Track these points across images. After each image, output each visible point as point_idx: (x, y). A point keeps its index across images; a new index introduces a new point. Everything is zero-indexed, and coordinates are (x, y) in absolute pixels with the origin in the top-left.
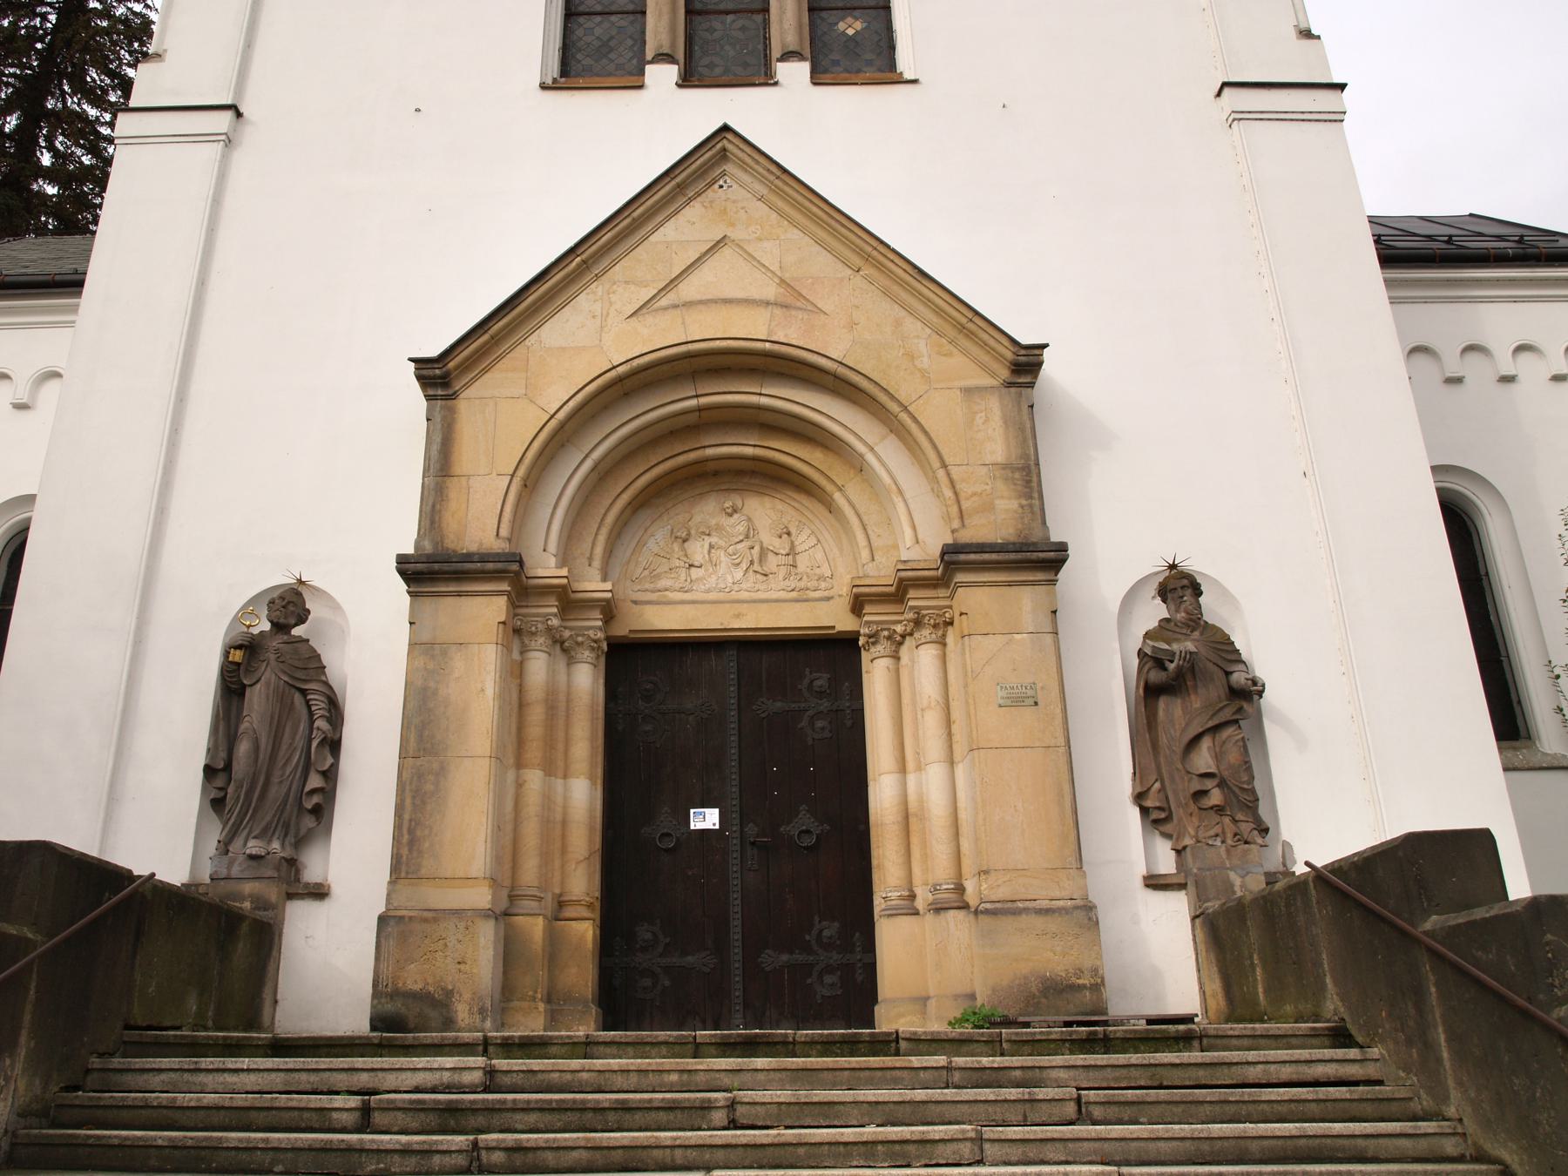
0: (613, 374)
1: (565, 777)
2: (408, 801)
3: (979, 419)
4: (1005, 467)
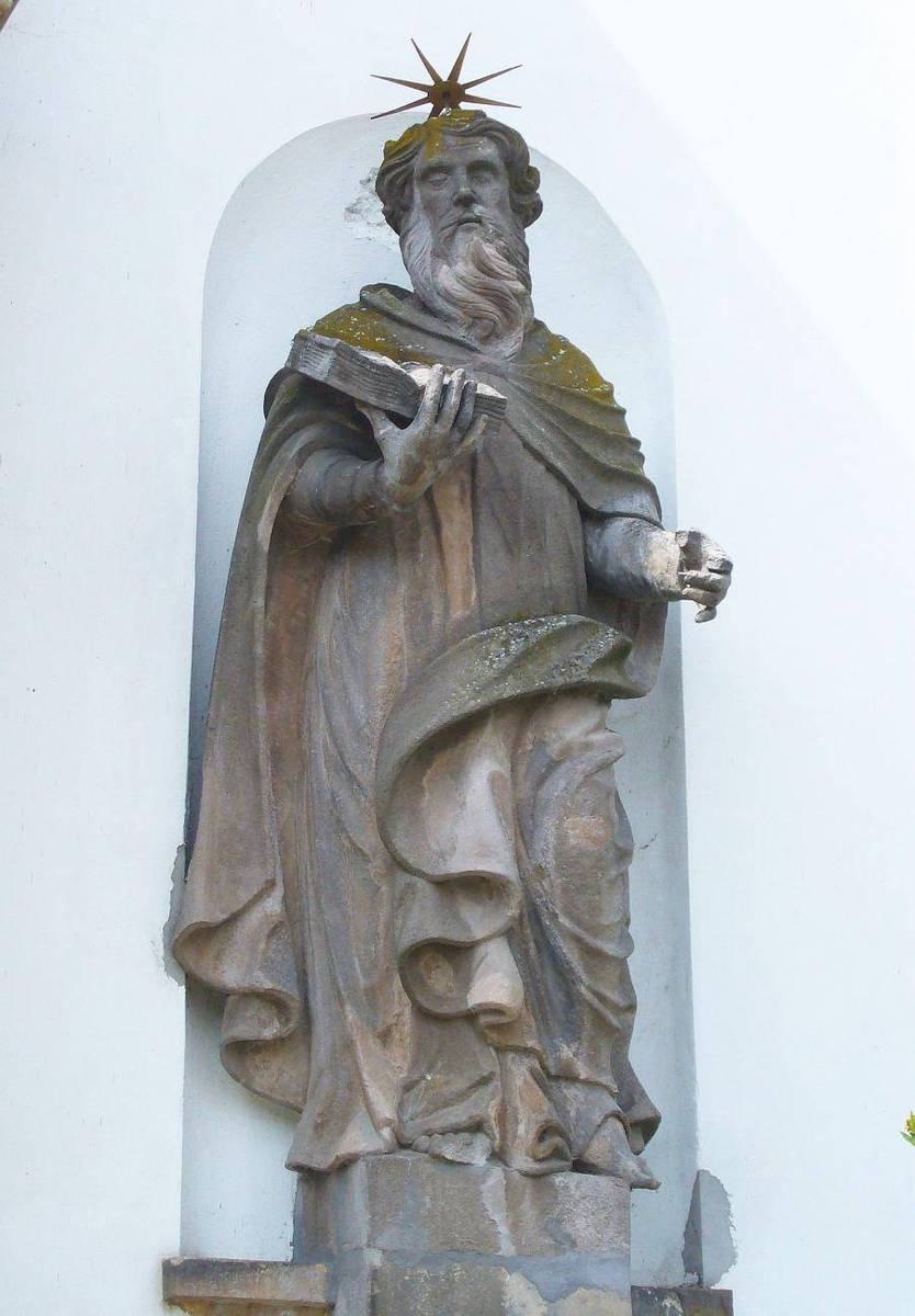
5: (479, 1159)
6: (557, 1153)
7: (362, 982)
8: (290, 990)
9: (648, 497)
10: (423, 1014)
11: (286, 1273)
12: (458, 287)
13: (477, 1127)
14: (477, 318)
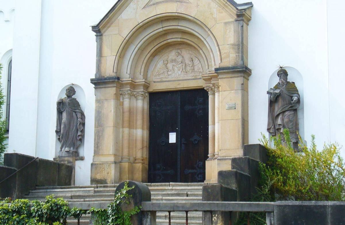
0: (139, 26)
1: (136, 129)
2: (96, 138)
3: (228, 31)
4: (233, 45)
8: (274, 132)
13: (282, 140)
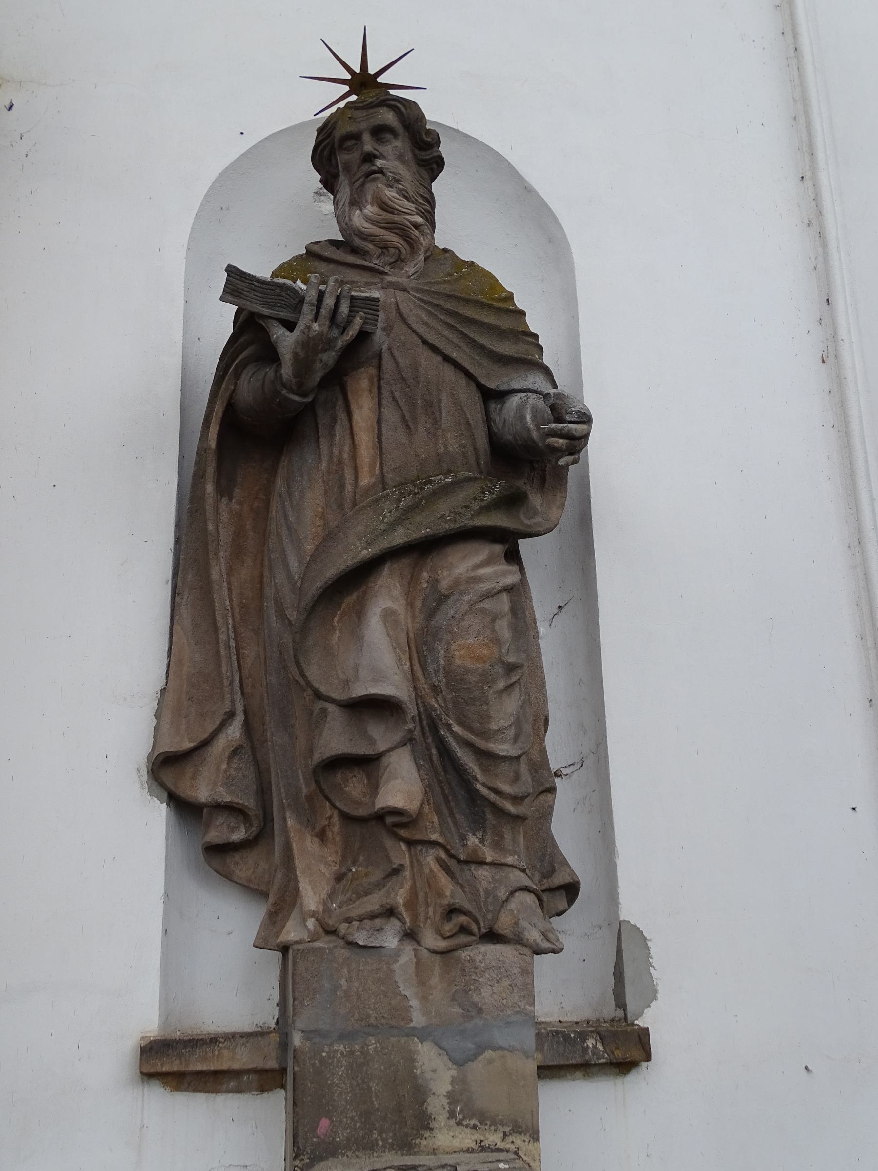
5: (390, 939)
6: (464, 930)
7: (305, 791)
8: (249, 802)
9: (542, 377)
10: (347, 818)
11: (243, 1044)
12: (366, 225)
13: (390, 912)
14: (384, 248)
